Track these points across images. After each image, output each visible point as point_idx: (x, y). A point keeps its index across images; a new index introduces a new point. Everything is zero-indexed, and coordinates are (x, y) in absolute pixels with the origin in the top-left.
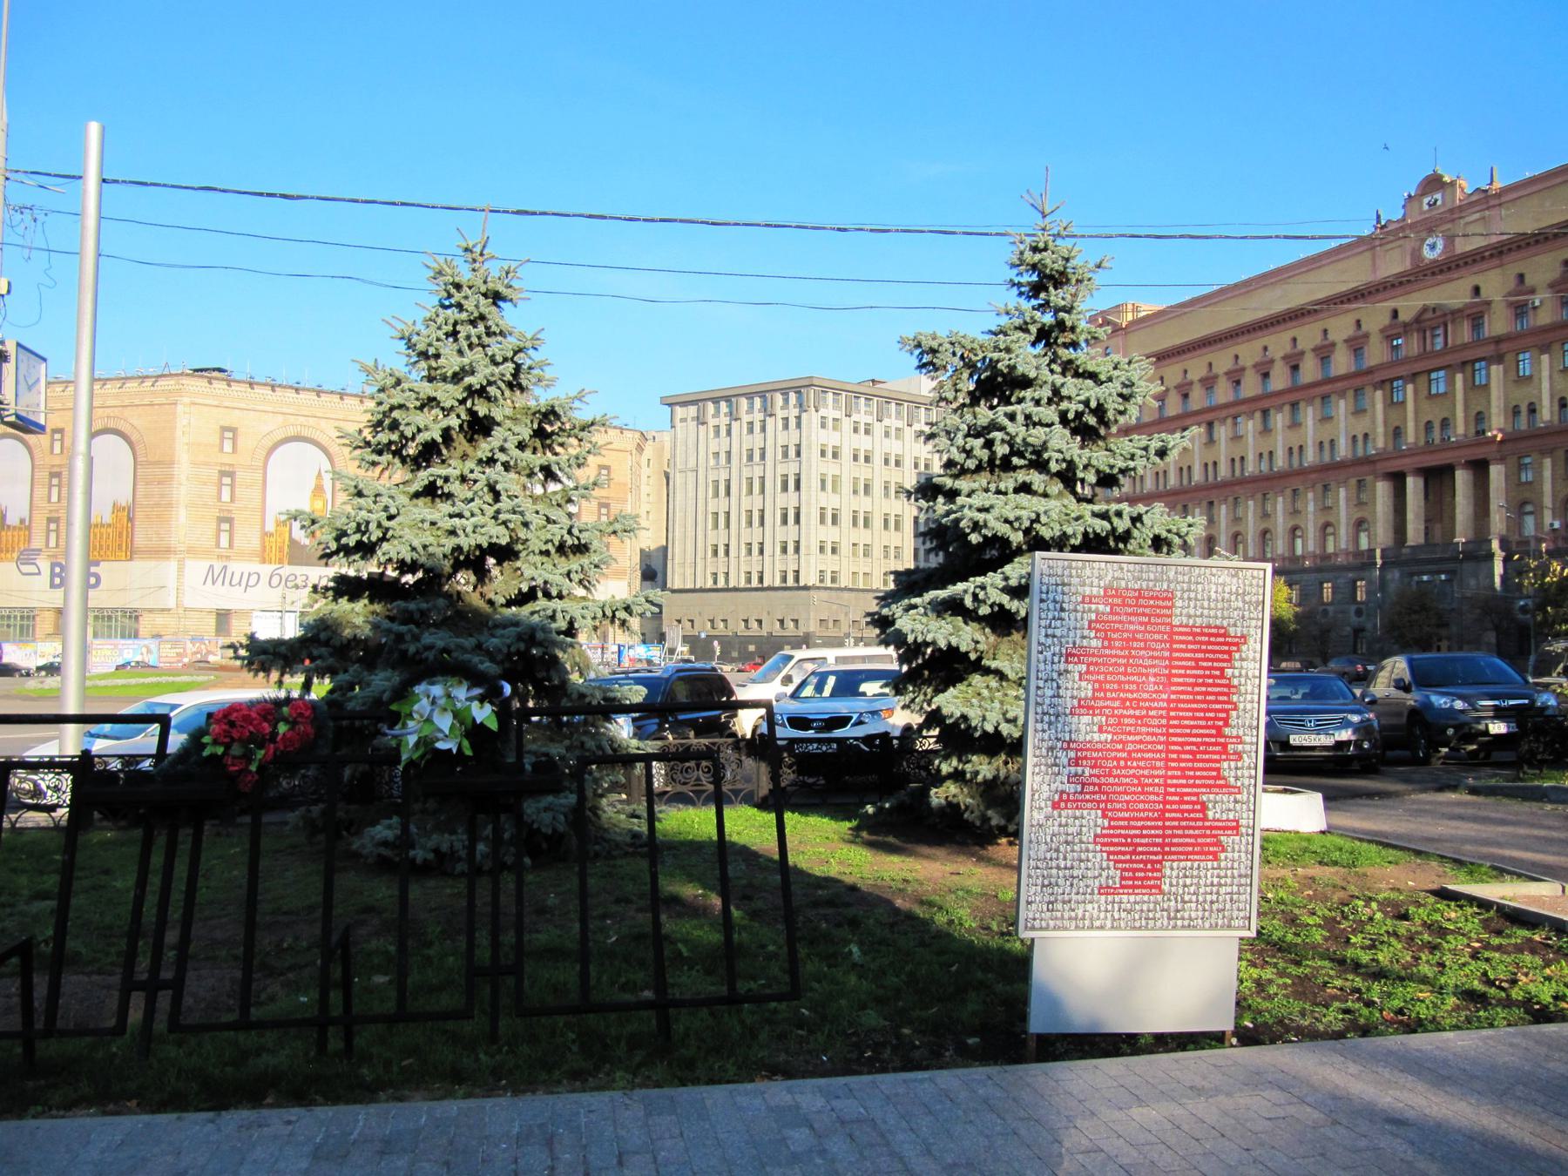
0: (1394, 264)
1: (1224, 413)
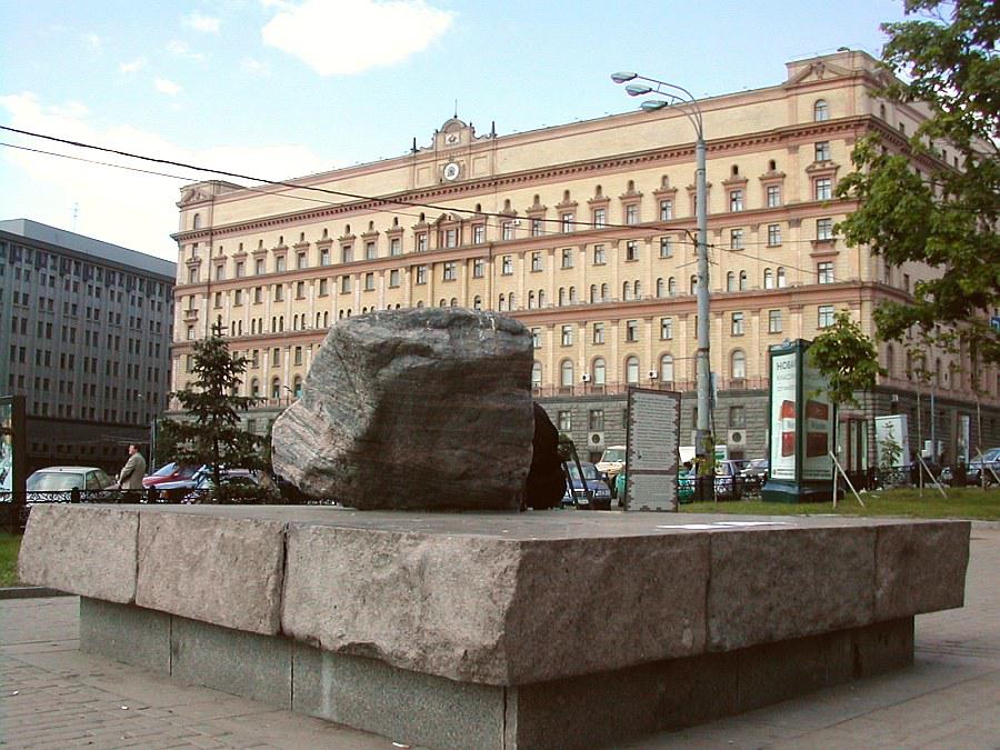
0: (426, 179)
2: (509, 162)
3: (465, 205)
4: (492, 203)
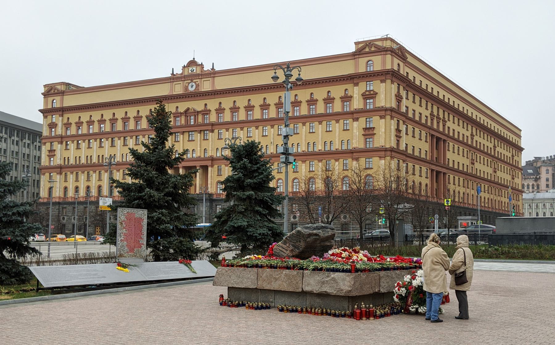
0: (178, 89)
2: (221, 84)
3: (198, 105)
4: (213, 104)
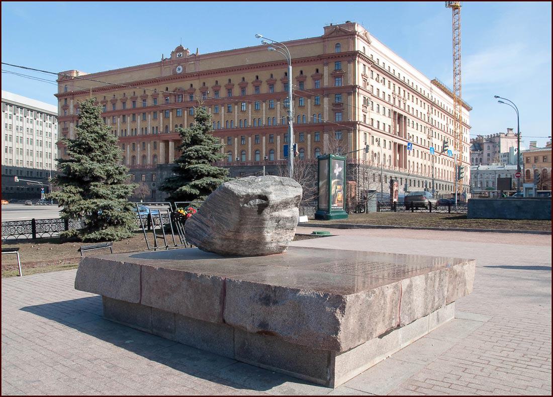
0: (167, 72)
1: (110, 114)
2: (203, 67)
3: (185, 85)
